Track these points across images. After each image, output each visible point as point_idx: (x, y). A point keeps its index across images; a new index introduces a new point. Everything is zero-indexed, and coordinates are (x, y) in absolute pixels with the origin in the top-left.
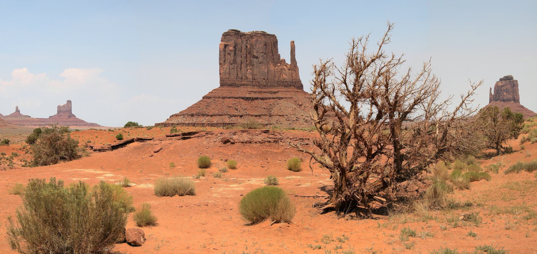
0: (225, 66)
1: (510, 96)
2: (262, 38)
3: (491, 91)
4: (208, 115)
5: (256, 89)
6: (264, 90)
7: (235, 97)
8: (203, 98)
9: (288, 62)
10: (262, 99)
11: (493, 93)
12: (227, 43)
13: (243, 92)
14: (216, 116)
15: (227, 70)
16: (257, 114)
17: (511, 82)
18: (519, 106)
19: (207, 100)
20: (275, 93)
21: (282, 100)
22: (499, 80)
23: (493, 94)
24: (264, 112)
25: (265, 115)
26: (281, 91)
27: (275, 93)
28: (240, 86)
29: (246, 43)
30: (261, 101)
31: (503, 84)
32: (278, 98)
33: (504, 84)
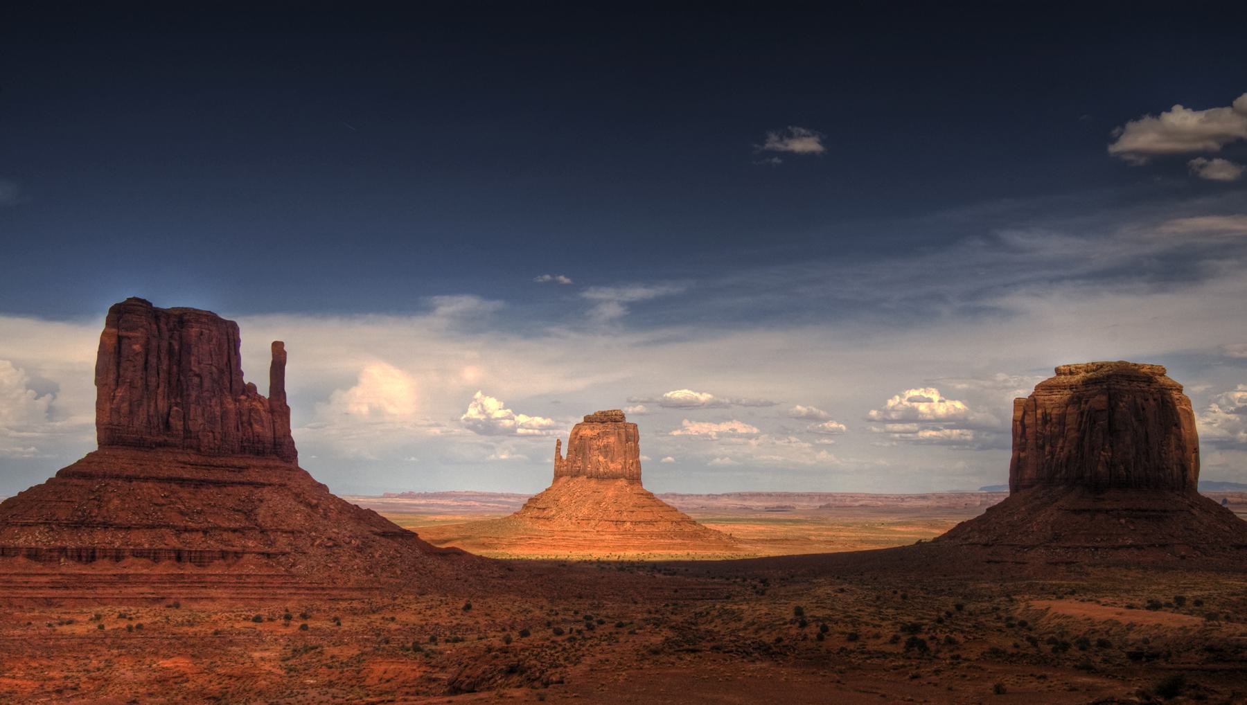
0: (119, 393)
1: (616, 466)
2: (211, 328)
3: (558, 450)
4: (120, 528)
5: (193, 458)
6: (213, 461)
7: (157, 479)
8: (63, 474)
9: (264, 390)
10: (219, 484)
11: (564, 457)
12: (124, 333)
13: (167, 463)
14: (141, 530)
15: (125, 406)
16: (233, 525)
17: (620, 428)
18: (642, 494)
19: (81, 482)
20: (241, 469)
21: (265, 490)
22: (583, 421)
23: (564, 457)
24: (239, 521)
25: (250, 529)
26: (257, 467)
27: (241, 469)
28: (154, 446)
29: (171, 337)
30: (214, 490)
31: (598, 431)
32: (251, 484)
33: (598, 434)
